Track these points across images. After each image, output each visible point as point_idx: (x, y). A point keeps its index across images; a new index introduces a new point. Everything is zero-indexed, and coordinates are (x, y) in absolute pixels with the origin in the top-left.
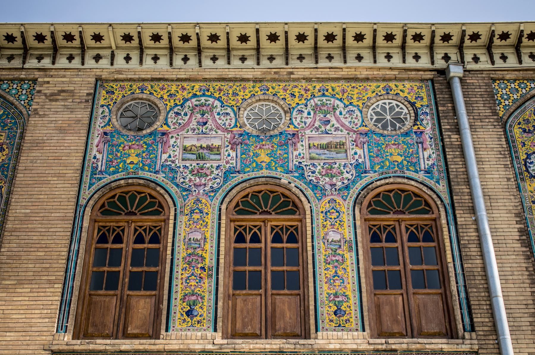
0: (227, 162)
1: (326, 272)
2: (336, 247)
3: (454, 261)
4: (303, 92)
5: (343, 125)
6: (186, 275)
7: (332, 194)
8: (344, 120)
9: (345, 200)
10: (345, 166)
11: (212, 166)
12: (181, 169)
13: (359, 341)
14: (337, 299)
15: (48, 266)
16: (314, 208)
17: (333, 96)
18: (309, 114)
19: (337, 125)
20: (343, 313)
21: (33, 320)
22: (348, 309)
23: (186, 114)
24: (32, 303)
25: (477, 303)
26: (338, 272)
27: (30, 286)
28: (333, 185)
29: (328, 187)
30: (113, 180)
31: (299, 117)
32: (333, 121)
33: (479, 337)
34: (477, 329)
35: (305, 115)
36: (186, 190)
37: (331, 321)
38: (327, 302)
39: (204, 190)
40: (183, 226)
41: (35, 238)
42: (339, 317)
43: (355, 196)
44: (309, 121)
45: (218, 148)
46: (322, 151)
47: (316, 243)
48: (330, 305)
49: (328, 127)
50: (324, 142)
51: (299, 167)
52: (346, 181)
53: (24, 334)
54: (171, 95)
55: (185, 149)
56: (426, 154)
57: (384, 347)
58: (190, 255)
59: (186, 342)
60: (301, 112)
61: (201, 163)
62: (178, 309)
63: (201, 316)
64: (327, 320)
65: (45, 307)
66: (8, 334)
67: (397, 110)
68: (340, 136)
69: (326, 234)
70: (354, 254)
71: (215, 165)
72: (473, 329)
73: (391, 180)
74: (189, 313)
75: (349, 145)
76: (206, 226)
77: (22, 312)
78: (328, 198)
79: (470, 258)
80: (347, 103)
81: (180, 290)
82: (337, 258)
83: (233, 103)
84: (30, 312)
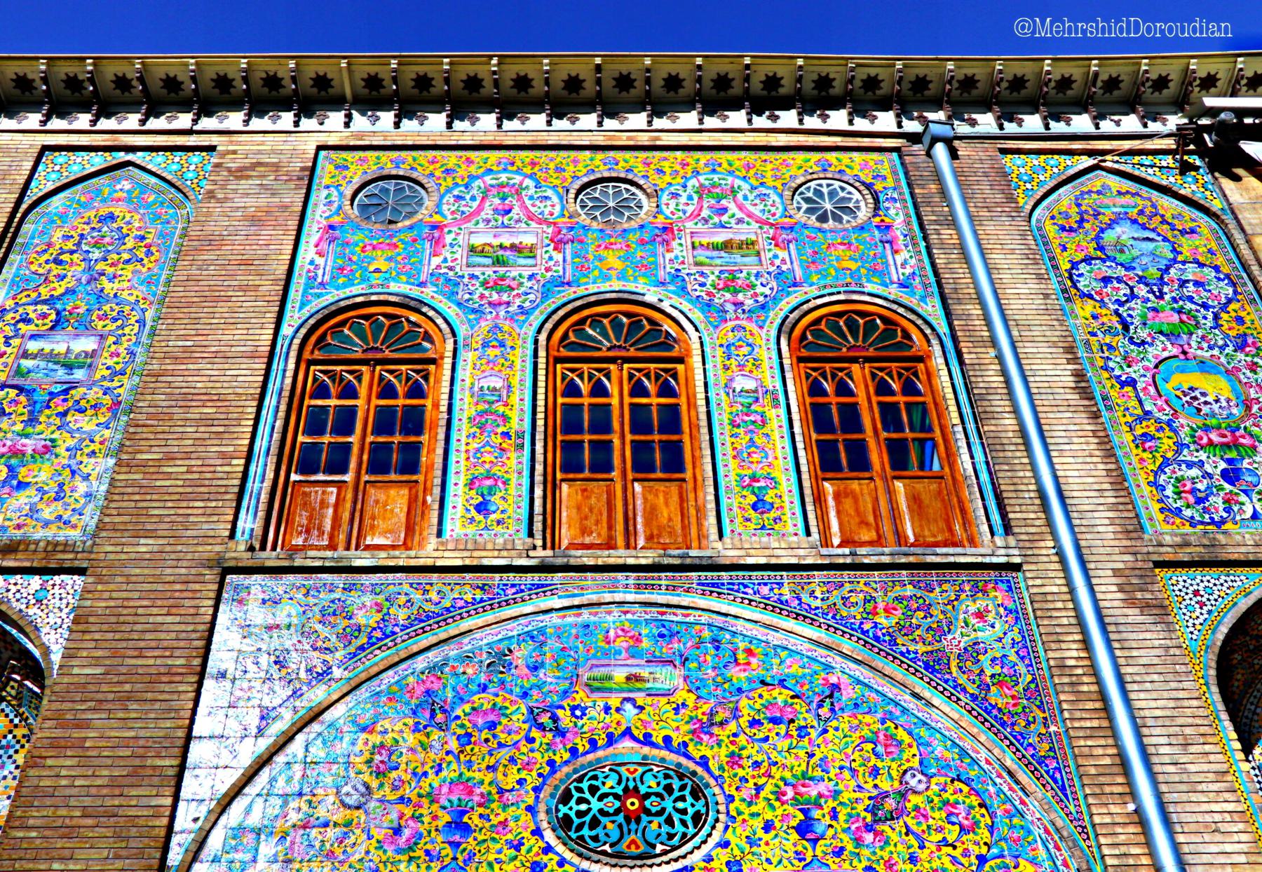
0: (547, 270)
1: (733, 440)
2: (750, 400)
3: (963, 422)
4: (678, 168)
5: (750, 215)
6: (474, 445)
7: (737, 318)
8: (752, 209)
9: (761, 327)
10: (757, 275)
11: (520, 276)
12: (466, 280)
13: (801, 552)
14: (757, 485)
15: (221, 429)
16: (706, 339)
17: (731, 173)
18: (690, 198)
19: (740, 215)
20: (768, 507)
21: (192, 519)
22: (778, 500)
23: (473, 198)
24: (189, 490)
25: (1012, 488)
26: (756, 439)
27: (187, 462)
28: (738, 304)
29: (729, 307)
30: (343, 296)
31: (673, 203)
32: (733, 208)
33: (1021, 544)
34: (1016, 530)
35: (683, 199)
36: (474, 311)
37: (748, 520)
38: (738, 489)
39: (507, 312)
40: (469, 367)
41: (199, 385)
42: (762, 513)
43: (778, 321)
44: (690, 209)
45: (531, 248)
46: (715, 254)
47: (712, 394)
48: (745, 493)
49: (725, 218)
50: (720, 238)
51: (677, 275)
52: (761, 299)
53: (172, 541)
54: (448, 172)
55: (473, 250)
56: (899, 258)
57: (849, 560)
58: (481, 414)
59: (476, 554)
60: (675, 195)
61: (502, 270)
62: (460, 502)
63: (502, 512)
64: (739, 520)
65: (212, 497)
66: (142, 541)
67: (842, 194)
68: (748, 231)
69: (731, 380)
70: (782, 411)
71: (526, 273)
72: (1008, 529)
73: (842, 297)
74: (482, 508)
75: (763, 243)
76: (511, 367)
77: (170, 504)
78: (730, 325)
79: (992, 416)
80: (754, 182)
81: (463, 469)
82: (752, 418)
83: (557, 182)
84: (184, 504)
